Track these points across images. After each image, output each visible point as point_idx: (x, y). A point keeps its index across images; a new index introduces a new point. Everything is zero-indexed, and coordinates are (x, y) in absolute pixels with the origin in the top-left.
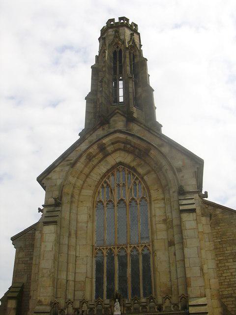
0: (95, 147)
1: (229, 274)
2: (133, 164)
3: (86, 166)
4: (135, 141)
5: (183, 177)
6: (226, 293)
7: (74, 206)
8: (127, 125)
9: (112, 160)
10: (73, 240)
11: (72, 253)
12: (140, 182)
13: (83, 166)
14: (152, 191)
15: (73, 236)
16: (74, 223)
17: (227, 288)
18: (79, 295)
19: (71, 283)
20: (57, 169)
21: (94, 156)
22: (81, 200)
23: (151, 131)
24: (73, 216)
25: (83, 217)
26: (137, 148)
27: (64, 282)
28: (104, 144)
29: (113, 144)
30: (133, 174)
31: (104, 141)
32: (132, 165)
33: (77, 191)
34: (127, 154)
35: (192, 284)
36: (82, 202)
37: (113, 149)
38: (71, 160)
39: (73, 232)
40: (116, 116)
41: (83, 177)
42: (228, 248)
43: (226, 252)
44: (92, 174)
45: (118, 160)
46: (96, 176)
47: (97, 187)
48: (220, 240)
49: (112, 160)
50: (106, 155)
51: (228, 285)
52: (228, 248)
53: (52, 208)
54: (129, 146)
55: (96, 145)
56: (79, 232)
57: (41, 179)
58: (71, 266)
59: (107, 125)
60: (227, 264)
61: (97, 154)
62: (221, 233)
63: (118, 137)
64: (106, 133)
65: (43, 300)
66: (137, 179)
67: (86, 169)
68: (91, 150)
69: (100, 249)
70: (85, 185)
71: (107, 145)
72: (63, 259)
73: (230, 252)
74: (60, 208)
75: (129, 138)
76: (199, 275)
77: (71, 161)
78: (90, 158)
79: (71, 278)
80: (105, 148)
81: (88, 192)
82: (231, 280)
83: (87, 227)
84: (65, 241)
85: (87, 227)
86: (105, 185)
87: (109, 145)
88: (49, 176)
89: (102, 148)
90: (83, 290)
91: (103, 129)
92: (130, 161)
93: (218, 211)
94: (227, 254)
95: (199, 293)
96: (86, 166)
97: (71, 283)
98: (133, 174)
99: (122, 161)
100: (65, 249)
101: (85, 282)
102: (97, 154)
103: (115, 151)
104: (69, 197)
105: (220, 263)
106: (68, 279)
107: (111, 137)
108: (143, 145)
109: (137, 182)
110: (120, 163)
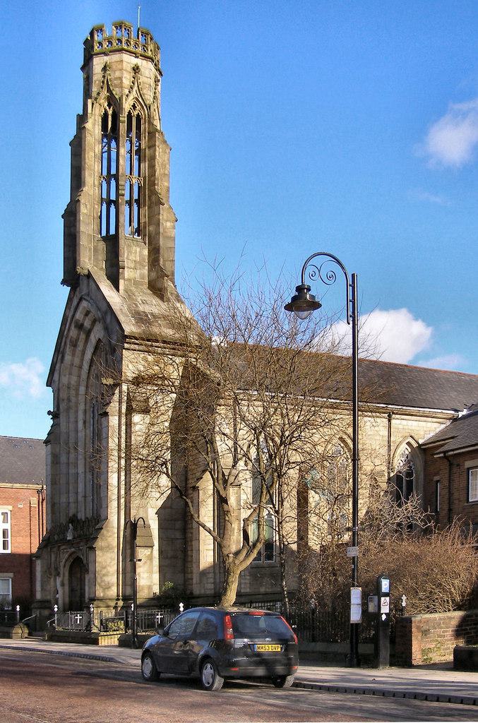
7: (72, 412)
10: (72, 456)
11: (72, 471)
15: (72, 451)
16: (72, 435)
33: (73, 392)
37: (90, 323)
41: (75, 370)
45: (97, 337)
50: (88, 333)
61: (79, 335)
68: (71, 334)
72: (63, 481)
84: (63, 459)
87: (84, 319)
100: (63, 468)
102: (79, 335)
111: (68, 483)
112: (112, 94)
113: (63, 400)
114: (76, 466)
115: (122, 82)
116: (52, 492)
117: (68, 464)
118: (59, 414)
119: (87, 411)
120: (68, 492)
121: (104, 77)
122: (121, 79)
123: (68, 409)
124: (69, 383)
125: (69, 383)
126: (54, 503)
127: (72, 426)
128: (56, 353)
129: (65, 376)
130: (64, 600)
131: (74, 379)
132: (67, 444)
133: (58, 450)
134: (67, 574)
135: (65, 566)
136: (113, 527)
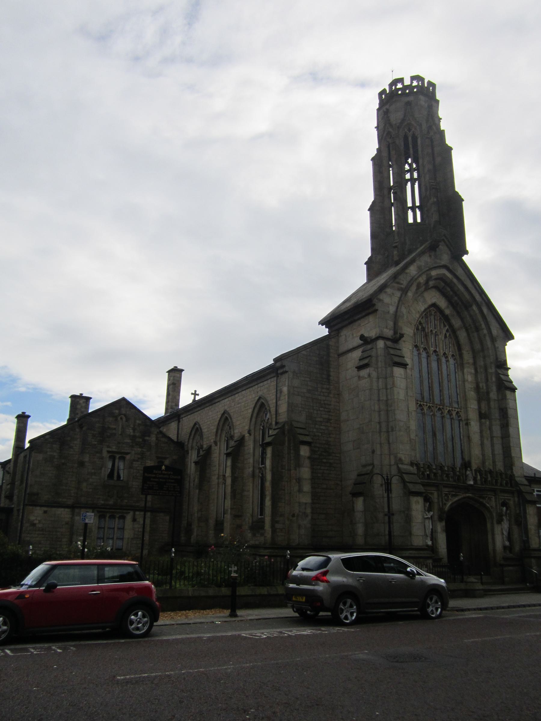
2: (447, 312)
14: (464, 352)
30: (443, 323)
38: (402, 284)
45: (434, 301)
63: (444, 274)
66: (447, 331)
75: (455, 281)
77: (402, 286)
86: (420, 327)
91: (430, 256)
109: (448, 335)
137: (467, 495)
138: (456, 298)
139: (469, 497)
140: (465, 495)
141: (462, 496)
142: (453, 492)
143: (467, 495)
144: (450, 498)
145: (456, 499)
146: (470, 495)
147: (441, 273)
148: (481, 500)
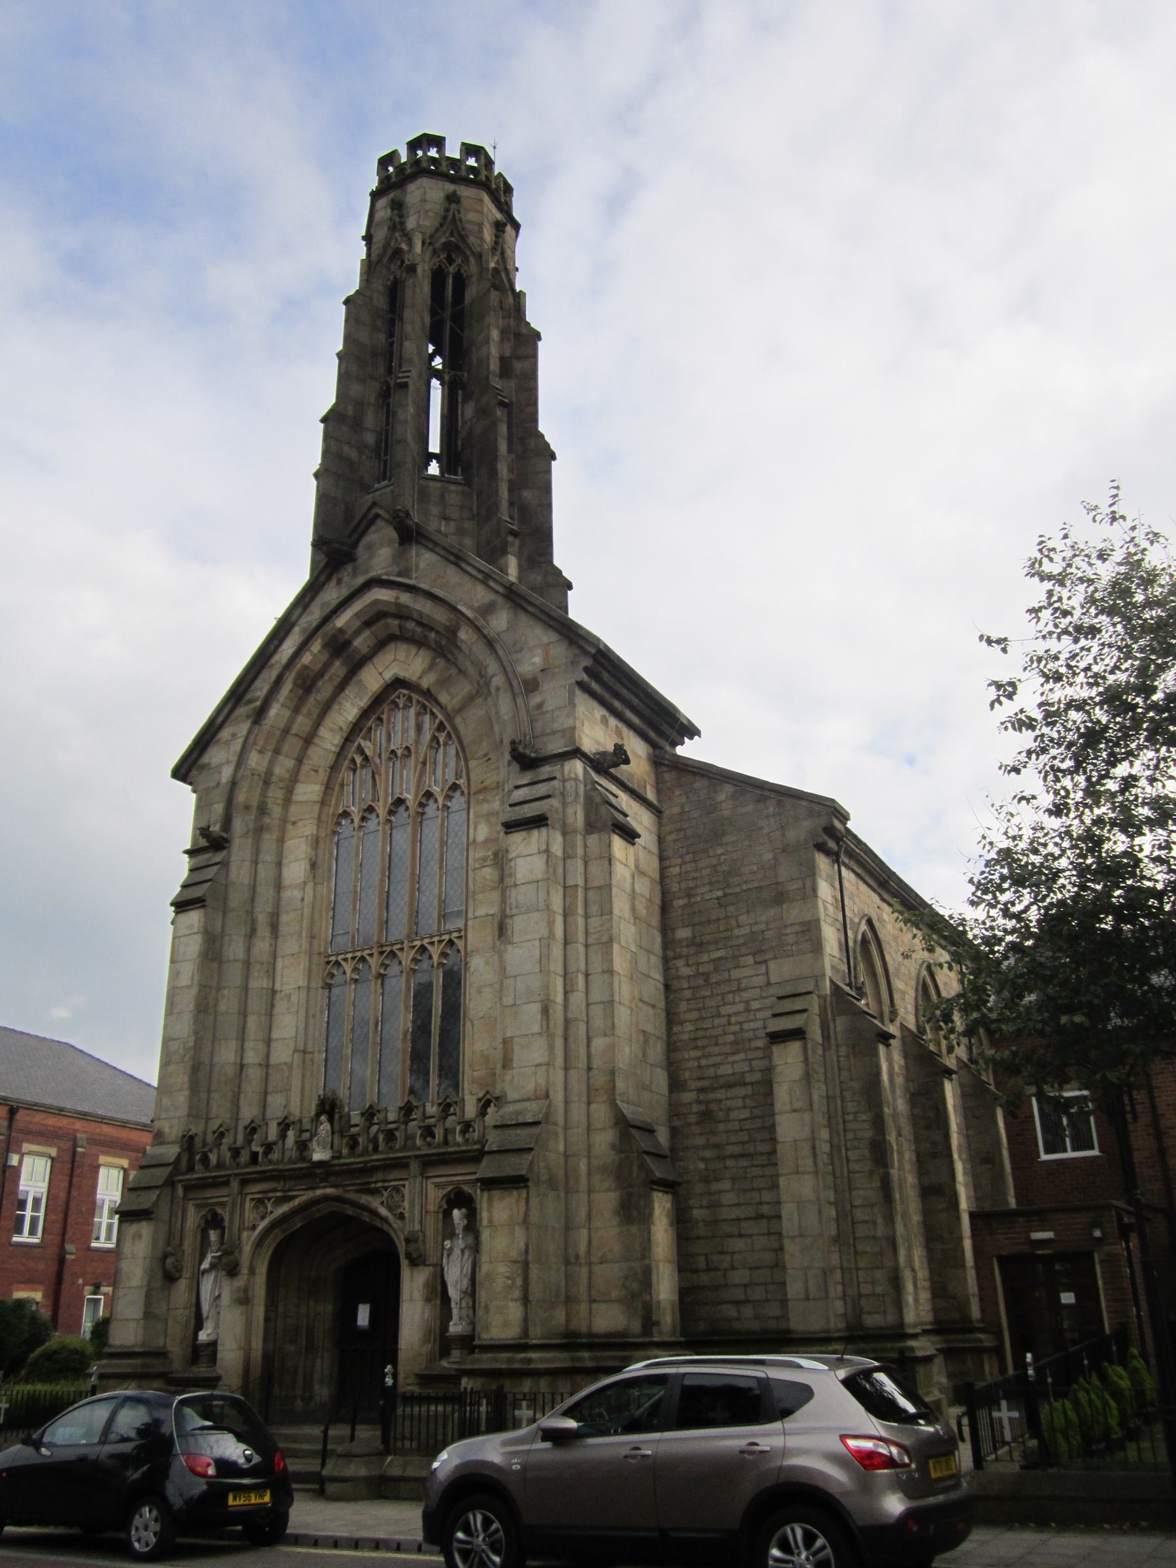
0: (316, 646)
1: (741, 1007)
3: (296, 711)
4: (423, 606)
5: (540, 706)
6: (726, 1070)
7: (269, 841)
8: (399, 557)
9: (373, 679)
10: (262, 946)
11: (258, 982)
12: (449, 736)
13: (287, 713)
15: (263, 931)
16: (266, 894)
17: (733, 1054)
18: (276, 1105)
19: (254, 1075)
20: (225, 734)
21: (321, 674)
22: (293, 819)
23: (463, 565)
24: (265, 872)
25: (296, 871)
26: (431, 629)
27: (230, 1071)
28: (341, 630)
29: (368, 624)
31: (340, 622)
32: (425, 683)
33: (276, 794)
34: (413, 650)
35: (515, 1058)
36: (294, 823)
37: (371, 643)
39: (262, 919)
40: (373, 528)
41: (292, 745)
42: (743, 919)
43: (736, 932)
44: (323, 732)
45: (388, 676)
46: (329, 739)
47: (334, 768)
48: (720, 893)
49: (373, 679)
50: (356, 666)
51: (736, 1042)
52: (743, 919)
53: (206, 856)
54: (411, 625)
55: (319, 641)
56: (284, 919)
57: (184, 771)
58: (252, 1021)
59: (349, 568)
60: (735, 974)
61: (327, 666)
62: (725, 868)
63: (376, 602)
64: (345, 592)
65: (166, 1130)
67: (300, 719)
68: (307, 659)
69: (337, 963)
70: (305, 768)
71: (350, 632)
72: (228, 1003)
73: (745, 931)
74: (224, 853)
75: (405, 598)
76: (536, 1028)
78: (307, 683)
79: (252, 1056)
80: (347, 643)
81: (309, 791)
82: (745, 1026)
83: (303, 899)
84: (235, 949)
85: (303, 899)
86: (359, 760)
87: (357, 633)
88: (205, 759)
89: (339, 646)
90: (287, 1090)
92: (418, 674)
93: (724, 793)
94: (737, 937)
95: (531, 1086)
96: (296, 711)
97: (254, 1075)
98: (432, 714)
99: (402, 674)
100: (234, 974)
101: (290, 1066)
102: (327, 666)
103: (380, 645)
104: (252, 816)
105: (716, 970)
106: (245, 1061)
107: (358, 605)
108: (440, 616)
109: (442, 738)
110: (398, 683)
111: (244, 1014)
112: (463, 238)
113: (247, 808)
114: (272, 973)
115: (481, 231)
116: (196, 1033)
117: (247, 964)
118: (227, 841)
119: (321, 841)
120: (242, 1038)
121: (447, 210)
122: (480, 225)
123: (259, 831)
124: (269, 772)
125: (269, 772)
126: (200, 1064)
127: (265, 872)
128: (233, 701)
129: (260, 752)
130: (247, 1350)
131: (284, 765)
132: (251, 913)
133: (219, 925)
134: (262, 1269)
135: (259, 1243)
136: (556, 1124)
137: (319, 1192)
138: (433, 635)
139: (325, 1199)
140: (309, 1195)
141: (304, 1198)
142: (275, 1190)
143: (319, 1192)
144: (270, 1208)
145: (285, 1208)
146: (330, 1191)
147: (368, 601)
148: (365, 1199)
